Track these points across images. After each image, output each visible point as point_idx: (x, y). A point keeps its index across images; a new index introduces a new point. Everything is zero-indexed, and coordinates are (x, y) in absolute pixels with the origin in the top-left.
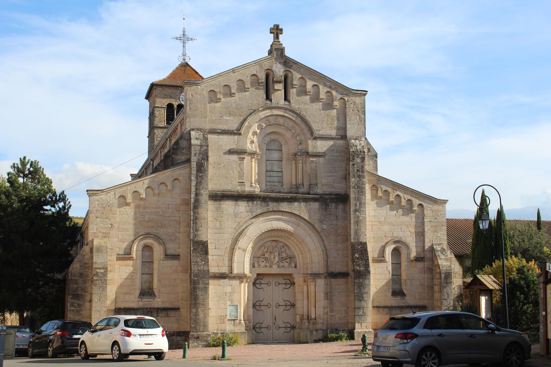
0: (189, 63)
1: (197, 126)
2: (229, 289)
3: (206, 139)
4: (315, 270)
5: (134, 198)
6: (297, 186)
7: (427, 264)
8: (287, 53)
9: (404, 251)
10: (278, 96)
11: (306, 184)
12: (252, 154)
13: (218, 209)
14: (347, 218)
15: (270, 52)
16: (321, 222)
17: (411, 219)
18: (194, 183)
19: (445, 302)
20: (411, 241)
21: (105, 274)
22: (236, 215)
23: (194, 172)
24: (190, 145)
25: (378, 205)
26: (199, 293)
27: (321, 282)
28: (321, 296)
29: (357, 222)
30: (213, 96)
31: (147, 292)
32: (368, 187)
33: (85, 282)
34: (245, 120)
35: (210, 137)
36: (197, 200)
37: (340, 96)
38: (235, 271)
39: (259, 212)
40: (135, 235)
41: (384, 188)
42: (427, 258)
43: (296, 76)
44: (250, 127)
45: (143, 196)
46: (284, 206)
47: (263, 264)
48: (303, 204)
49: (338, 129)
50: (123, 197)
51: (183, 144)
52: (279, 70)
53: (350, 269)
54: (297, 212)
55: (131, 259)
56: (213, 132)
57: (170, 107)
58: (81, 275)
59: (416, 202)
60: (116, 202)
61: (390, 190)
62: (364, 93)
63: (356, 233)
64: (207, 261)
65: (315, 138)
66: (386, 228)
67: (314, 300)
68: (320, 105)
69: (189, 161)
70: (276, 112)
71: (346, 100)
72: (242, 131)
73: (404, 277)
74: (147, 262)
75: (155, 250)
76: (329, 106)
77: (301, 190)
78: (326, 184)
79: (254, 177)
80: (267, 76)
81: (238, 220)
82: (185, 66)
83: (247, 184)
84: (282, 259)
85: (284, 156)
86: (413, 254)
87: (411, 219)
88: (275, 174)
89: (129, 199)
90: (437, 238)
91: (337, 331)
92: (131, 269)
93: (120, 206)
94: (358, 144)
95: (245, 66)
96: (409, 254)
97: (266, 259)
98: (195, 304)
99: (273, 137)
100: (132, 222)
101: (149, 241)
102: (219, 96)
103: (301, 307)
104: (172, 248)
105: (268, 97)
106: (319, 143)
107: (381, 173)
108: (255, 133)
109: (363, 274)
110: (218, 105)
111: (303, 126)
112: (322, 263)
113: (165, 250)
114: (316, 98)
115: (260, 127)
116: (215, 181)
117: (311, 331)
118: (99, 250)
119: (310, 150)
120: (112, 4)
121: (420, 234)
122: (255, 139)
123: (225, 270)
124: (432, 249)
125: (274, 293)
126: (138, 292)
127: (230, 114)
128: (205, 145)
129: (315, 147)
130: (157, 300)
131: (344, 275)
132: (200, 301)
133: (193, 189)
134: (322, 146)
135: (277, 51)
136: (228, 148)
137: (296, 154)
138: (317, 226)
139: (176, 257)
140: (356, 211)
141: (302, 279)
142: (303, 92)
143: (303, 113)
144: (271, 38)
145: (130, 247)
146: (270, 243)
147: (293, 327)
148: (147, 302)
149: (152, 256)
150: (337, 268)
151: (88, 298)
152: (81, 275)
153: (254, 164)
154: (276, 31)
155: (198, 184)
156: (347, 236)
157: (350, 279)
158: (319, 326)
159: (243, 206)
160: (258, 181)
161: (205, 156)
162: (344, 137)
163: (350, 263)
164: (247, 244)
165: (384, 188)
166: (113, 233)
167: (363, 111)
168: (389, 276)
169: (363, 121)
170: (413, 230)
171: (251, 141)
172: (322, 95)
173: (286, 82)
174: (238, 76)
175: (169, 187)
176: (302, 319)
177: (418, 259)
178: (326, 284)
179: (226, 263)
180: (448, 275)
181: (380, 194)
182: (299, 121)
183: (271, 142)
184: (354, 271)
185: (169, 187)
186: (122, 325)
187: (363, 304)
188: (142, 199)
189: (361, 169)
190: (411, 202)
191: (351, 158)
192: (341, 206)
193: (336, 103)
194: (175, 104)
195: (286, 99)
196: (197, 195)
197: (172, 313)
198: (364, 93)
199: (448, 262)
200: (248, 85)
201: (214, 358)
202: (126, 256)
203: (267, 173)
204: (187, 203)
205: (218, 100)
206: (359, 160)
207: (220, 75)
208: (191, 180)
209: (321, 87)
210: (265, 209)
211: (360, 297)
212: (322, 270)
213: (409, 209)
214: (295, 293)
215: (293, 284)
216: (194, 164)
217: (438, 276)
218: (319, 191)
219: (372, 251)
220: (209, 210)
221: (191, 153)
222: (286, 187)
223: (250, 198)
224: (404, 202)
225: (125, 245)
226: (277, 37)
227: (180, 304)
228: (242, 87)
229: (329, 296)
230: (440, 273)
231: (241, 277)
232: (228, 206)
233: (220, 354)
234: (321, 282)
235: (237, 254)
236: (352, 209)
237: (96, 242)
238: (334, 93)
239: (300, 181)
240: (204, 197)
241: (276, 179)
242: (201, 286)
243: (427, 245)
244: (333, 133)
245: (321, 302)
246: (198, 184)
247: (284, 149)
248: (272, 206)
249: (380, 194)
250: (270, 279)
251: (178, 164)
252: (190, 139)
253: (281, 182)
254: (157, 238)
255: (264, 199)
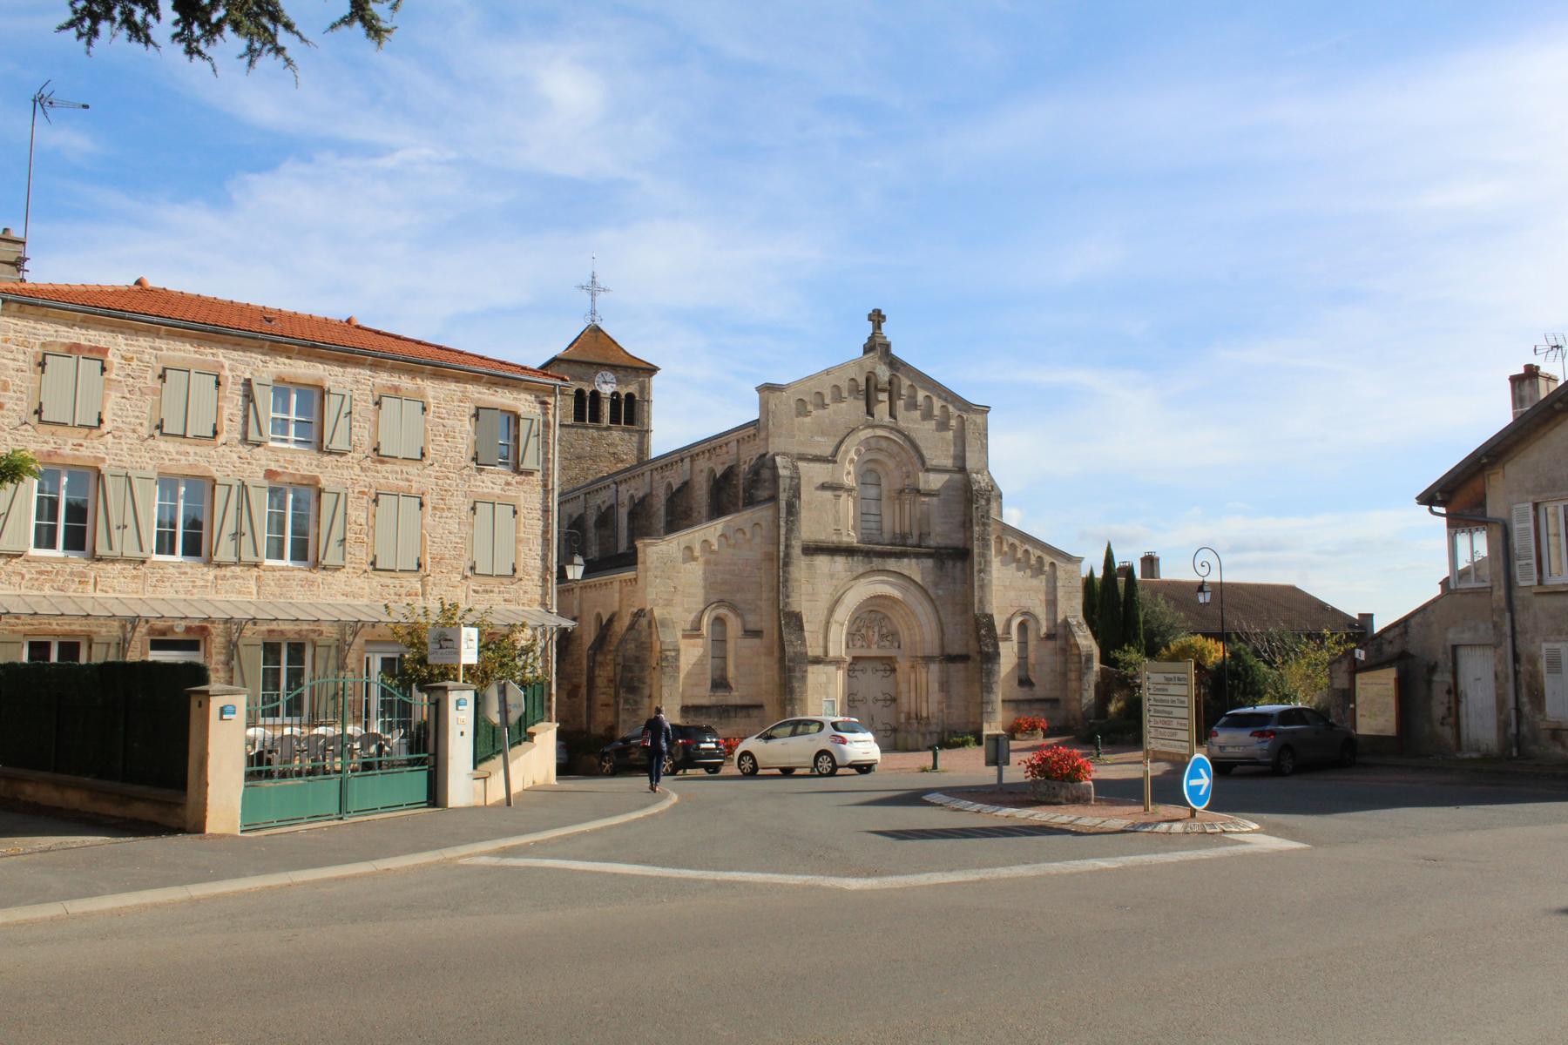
0: (602, 327)
1: (782, 448)
2: (823, 678)
3: (796, 468)
4: (928, 652)
5: (703, 550)
6: (904, 536)
7: (1059, 643)
8: (894, 351)
9: (1031, 625)
10: (882, 410)
11: (916, 533)
12: (849, 490)
13: (810, 567)
14: (968, 580)
15: (868, 349)
16: (936, 585)
17: (1040, 583)
18: (783, 531)
19: (1086, 694)
20: (1041, 612)
21: (677, 658)
22: (832, 576)
23: (783, 514)
24: (775, 478)
25: (1004, 563)
26: (796, 685)
27: (935, 668)
28: (935, 687)
29: (982, 587)
30: (802, 408)
31: (720, 683)
32: (993, 538)
33: (642, 670)
34: (841, 442)
35: (801, 465)
36: (787, 555)
37: (957, 413)
38: (831, 654)
39: (861, 571)
40: (706, 600)
41: (1011, 540)
42: (1060, 635)
43: (905, 382)
44: (847, 452)
45: (715, 547)
46: (892, 564)
47: (859, 644)
48: (914, 561)
49: (955, 457)
50: (689, 548)
51: (766, 474)
52: (883, 373)
53: (970, 650)
54: (906, 573)
55: (699, 636)
56: (803, 458)
57: (580, 393)
58: (637, 660)
59: (1048, 559)
60: (680, 555)
61: (1017, 542)
62: (984, 410)
63: (981, 601)
64: (803, 641)
65: (928, 470)
66: (1012, 594)
67: (926, 692)
68: (932, 425)
69: (774, 498)
70: (880, 432)
71: (963, 419)
72: (838, 458)
73: (1032, 659)
74: (719, 641)
75: (729, 624)
76: (943, 425)
77: (910, 542)
78: (941, 533)
79: (851, 522)
80: (868, 380)
81: (835, 582)
82: (595, 332)
83: (844, 532)
84: (883, 637)
85: (885, 494)
86: (1044, 630)
87: (1040, 583)
88: (872, 518)
89: (697, 553)
90: (1072, 607)
91: (955, 733)
92: (701, 650)
93: (685, 562)
94: (980, 480)
95: (841, 367)
96: (1038, 630)
97: (863, 637)
98: (791, 700)
99: (871, 466)
100: (702, 583)
101: (722, 611)
102: (810, 408)
103: (907, 702)
104: (753, 622)
105: (870, 412)
106: (932, 476)
107: (1006, 520)
108: (852, 461)
109: (992, 657)
110: (808, 419)
111: (912, 453)
112: (937, 643)
113: (744, 626)
114: (928, 415)
115: (858, 452)
116: (810, 528)
117: (924, 735)
118: (664, 624)
119: (922, 486)
120: (254, 177)
121: (1052, 603)
122: (851, 469)
123: (819, 652)
124: (1066, 623)
125: (874, 684)
126: (709, 683)
127: (823, 434)
128: (796, 477)
129: (926, 482)
130: (735, 694)
131: (963, 658)
132: (798, 695)
133: (782, 539)
134: (935, 481)
135: (876, 346)
136: (820, 481)
137: (901, 491)
138: (931, 591)
139: (756, 634)
140: (980, 571)
141: (908, 664)
142: (912, 405)
143: (913, 435)
144: (868, 328)
145: (700, 620)
146: (873, 615)
147: (895, 730)
148: (721, 698)
149: (724, 632)
150: (956, 649)
151: (646, 692)
152: (637, 660)
153: (851, 504)
154: (877, 318)
155: (789, 531)
156: (967, 605)
157: (971, 664)
158: (933, 728)
159: (840, 563)
160: (854, 528)
161: (796, 492)
162: (962, 469)
163: (973, 643)
164: (843, 614)
165: (1011, 540)
166: (677, 599)
167: (983, 434)
168: (1015, 660)
169: (984, 448)
170: (1043, 597)
171: (847, 474)
172: (936, 412)
173: (892, 390)
174: (832, 380)
175: (748, 535)
176: (909, 717)
177: (1050, 636)
178: (942, 671)
179: (821, 642)
180: (1089, 658)
181: (1005, 548)
182: (907, 445)
183: (869, 473)
184: (980, 652)
185: (748, 535)
186: (828, 729)
187: (993, 697)
188: (713, 552)
189: (986, 515)
190: (1041, 558)
191: (972, 498)
192: (959, 565)
193: (953, 422)
194: (588, 390)
195: (892, 415)
196: (787, 546)
197: (755, 713)
198: (984, 410)
199: (1086, 640)
200: (845, 394)
201: (924, 770)
202: (694, 631)
203: (863, 515)
204: (771, 557)
205: (808, 414)
206: (983, 502)
207: (810, 378)
208: (779, 527)
209: (935, 399)
210: (868, 568)
211: (988, 688)
212: (936, 652)
213: (1038, 570)
214: (897, 684)
215: (894, 670)
216: (783, 504)
217: (1076, 659)
218: (932, 543)
219: (999, 630)
220: (801, 567)
221: (777, 488)
222: (887, 537)
223: (849, 551)
224: (1033, 561)
225: (692, 617)
226: (877, 326)
227: (764, 699)
228: (838, 398)
229: (945, 686)
230: (1080, 655)
231: (837, 662)
232: (822, 561)
233: (930, 763)
234: (935, 668)
235: (834, 628)
236: (976, 568)
237: (657, 613)
238: (951, 408)
239: (907, 529)
240: (796, 551)
241: (874, 525)
242: (798, 674)
243: (1060, 618)
244: (949, 463)
245: (935, 696)
246: (789, 531)
247: (884, 483)
248: (877, 563)
249: (1005, 548)
250: (868, 665)
251: (759, 503)
252: (774, 468)
253: (881, 530)
254: (733, 608)
255: (868, 554)
